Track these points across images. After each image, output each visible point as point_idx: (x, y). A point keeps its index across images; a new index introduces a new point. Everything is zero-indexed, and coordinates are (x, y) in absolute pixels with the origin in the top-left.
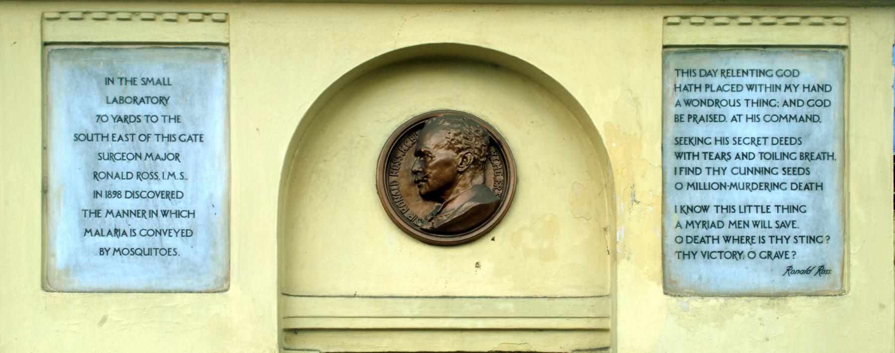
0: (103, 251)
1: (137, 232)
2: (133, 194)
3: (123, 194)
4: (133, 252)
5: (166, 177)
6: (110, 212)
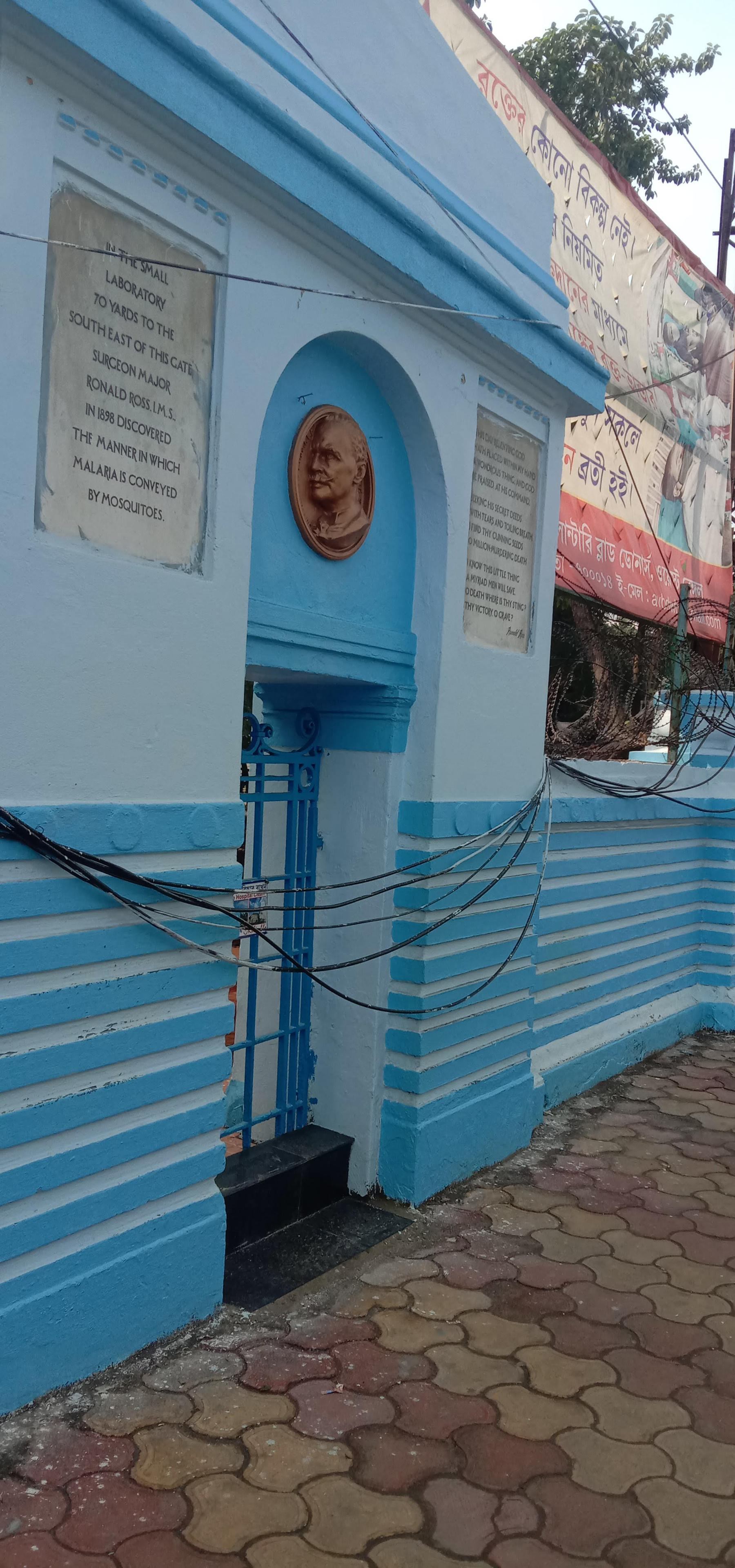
0: (92, 495)
1: (127, 476)
2: (125, 422)
3: (116, 417)
4: (122, 504)
5: (156, 410)
6: (101, 440)
